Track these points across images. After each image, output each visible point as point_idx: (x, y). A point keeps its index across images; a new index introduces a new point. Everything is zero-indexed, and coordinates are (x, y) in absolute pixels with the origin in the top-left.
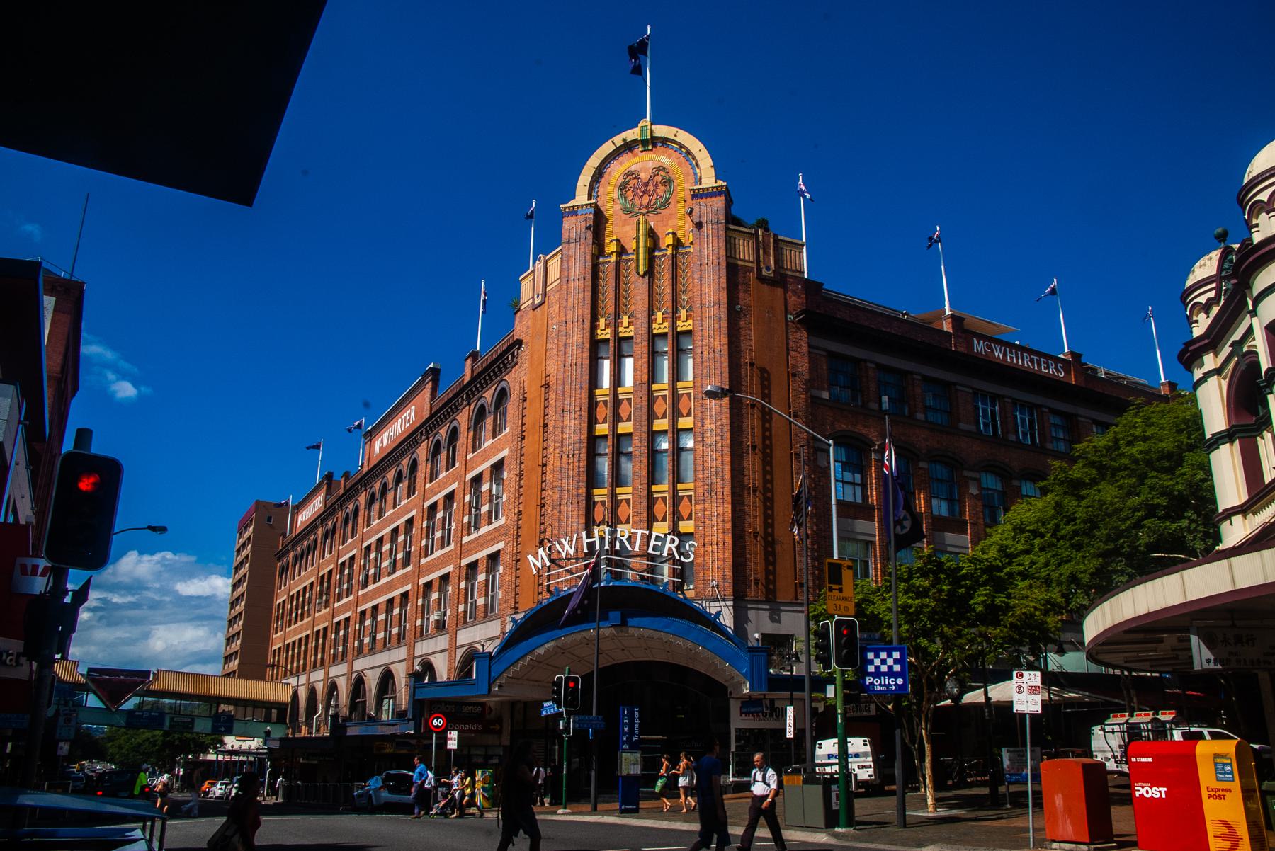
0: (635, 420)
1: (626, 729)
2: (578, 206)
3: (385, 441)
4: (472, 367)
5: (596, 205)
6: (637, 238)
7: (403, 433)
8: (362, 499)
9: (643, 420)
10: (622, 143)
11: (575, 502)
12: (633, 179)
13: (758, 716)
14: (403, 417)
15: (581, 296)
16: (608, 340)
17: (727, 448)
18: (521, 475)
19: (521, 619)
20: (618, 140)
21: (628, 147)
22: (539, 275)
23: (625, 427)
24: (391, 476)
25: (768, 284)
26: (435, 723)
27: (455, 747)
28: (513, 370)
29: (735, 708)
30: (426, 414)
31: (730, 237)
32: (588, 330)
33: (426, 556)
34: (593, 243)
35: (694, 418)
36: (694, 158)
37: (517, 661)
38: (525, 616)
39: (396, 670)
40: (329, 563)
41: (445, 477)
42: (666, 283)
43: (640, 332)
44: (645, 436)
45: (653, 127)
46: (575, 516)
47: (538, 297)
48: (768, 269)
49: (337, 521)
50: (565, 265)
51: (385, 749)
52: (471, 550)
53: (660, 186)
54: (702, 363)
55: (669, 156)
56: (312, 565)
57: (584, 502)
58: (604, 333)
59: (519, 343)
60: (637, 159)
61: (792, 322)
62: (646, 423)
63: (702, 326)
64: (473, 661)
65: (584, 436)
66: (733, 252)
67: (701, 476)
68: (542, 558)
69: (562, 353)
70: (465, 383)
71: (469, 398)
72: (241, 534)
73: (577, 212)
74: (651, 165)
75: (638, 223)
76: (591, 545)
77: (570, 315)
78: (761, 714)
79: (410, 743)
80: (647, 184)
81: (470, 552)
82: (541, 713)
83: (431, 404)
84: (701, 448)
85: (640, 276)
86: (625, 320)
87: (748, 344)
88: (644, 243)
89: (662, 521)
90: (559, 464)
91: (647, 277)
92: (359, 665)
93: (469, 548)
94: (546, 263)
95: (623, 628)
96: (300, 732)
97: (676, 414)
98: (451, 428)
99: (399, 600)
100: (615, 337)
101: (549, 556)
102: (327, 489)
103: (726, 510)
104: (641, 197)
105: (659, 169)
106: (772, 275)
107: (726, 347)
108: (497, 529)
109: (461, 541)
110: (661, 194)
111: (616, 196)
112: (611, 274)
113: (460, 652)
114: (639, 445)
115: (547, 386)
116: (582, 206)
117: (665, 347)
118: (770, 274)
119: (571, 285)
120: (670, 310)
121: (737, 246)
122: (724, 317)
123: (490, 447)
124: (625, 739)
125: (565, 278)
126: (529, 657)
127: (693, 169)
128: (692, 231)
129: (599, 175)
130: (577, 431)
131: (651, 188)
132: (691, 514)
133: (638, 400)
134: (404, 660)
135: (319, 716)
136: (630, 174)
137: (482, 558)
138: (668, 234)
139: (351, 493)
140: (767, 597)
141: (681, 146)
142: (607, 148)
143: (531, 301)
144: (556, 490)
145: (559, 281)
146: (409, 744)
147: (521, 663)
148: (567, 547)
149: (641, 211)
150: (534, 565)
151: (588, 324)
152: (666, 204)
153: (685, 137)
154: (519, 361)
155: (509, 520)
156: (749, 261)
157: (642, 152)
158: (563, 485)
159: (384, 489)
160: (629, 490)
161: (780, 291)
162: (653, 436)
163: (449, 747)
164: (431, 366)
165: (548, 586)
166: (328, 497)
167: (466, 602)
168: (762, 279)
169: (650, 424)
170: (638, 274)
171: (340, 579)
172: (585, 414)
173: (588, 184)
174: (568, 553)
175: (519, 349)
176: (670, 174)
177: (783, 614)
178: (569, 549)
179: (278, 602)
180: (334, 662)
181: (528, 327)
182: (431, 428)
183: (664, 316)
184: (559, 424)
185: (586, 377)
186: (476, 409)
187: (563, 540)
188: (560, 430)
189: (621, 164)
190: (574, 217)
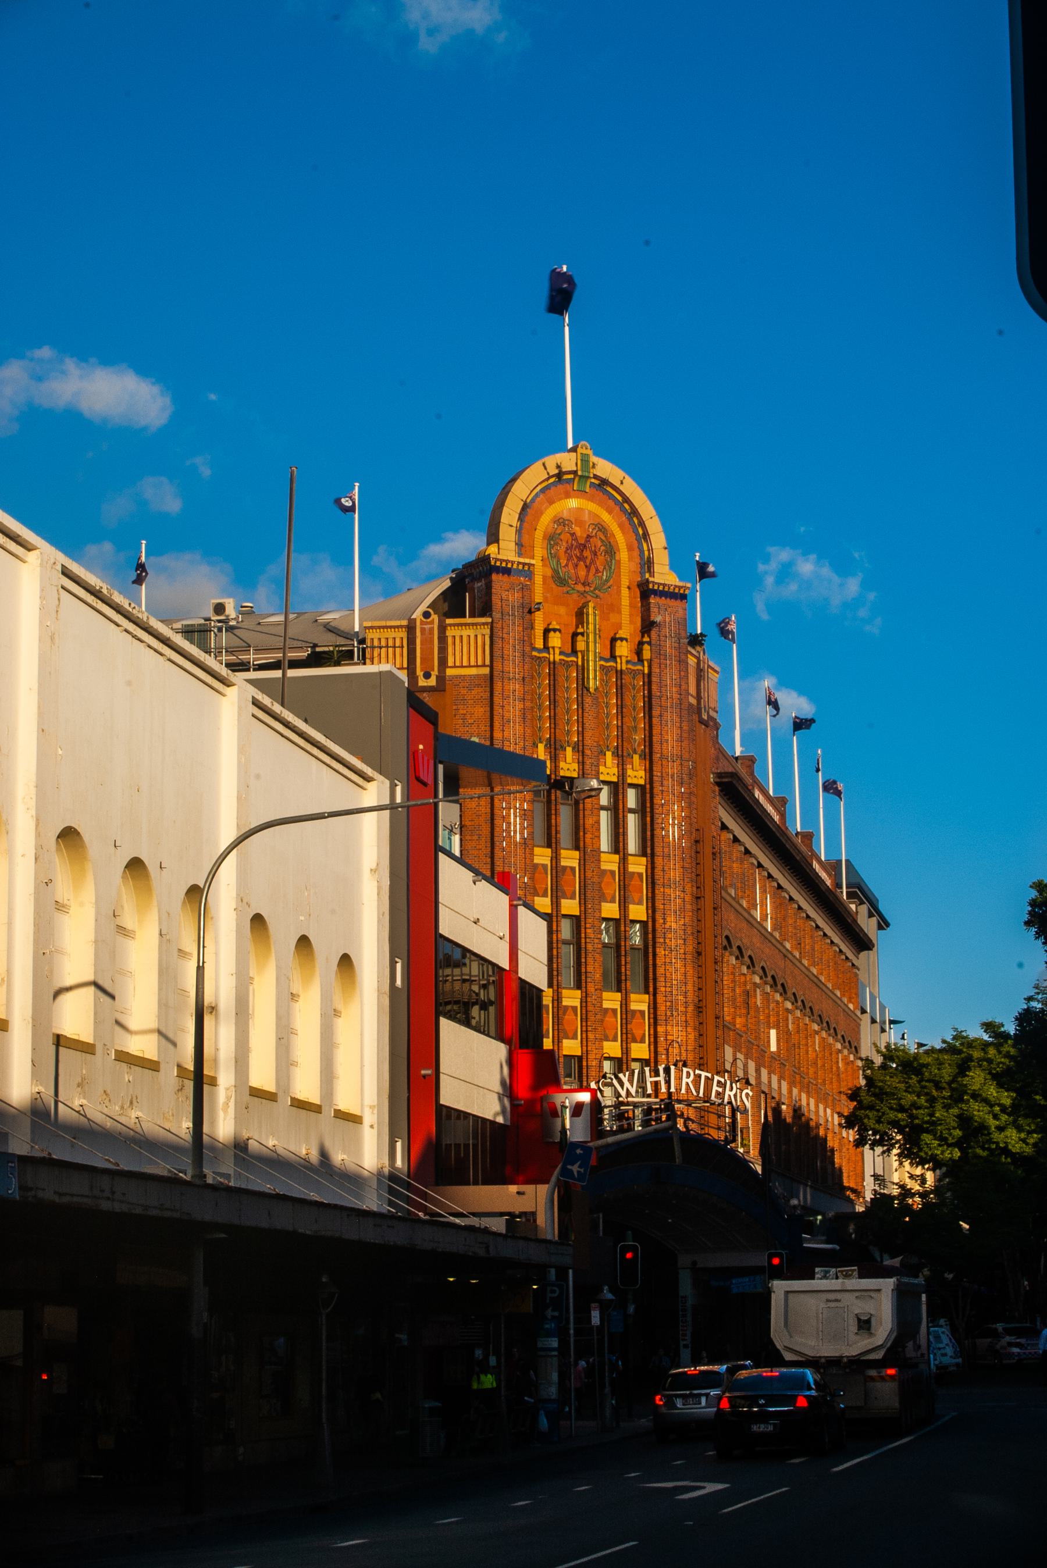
22: (427, 642)
36: (642, 524)
47: (427, 676)
84: (663, 952)
89: (612, 1041)
110: (601, 568)
131: (587, 553)
136: (560, 521)
141: (626, 500)
148: (627, 1084)
153: (632, 489)
187: (621, 1075)
190: (505, 578)
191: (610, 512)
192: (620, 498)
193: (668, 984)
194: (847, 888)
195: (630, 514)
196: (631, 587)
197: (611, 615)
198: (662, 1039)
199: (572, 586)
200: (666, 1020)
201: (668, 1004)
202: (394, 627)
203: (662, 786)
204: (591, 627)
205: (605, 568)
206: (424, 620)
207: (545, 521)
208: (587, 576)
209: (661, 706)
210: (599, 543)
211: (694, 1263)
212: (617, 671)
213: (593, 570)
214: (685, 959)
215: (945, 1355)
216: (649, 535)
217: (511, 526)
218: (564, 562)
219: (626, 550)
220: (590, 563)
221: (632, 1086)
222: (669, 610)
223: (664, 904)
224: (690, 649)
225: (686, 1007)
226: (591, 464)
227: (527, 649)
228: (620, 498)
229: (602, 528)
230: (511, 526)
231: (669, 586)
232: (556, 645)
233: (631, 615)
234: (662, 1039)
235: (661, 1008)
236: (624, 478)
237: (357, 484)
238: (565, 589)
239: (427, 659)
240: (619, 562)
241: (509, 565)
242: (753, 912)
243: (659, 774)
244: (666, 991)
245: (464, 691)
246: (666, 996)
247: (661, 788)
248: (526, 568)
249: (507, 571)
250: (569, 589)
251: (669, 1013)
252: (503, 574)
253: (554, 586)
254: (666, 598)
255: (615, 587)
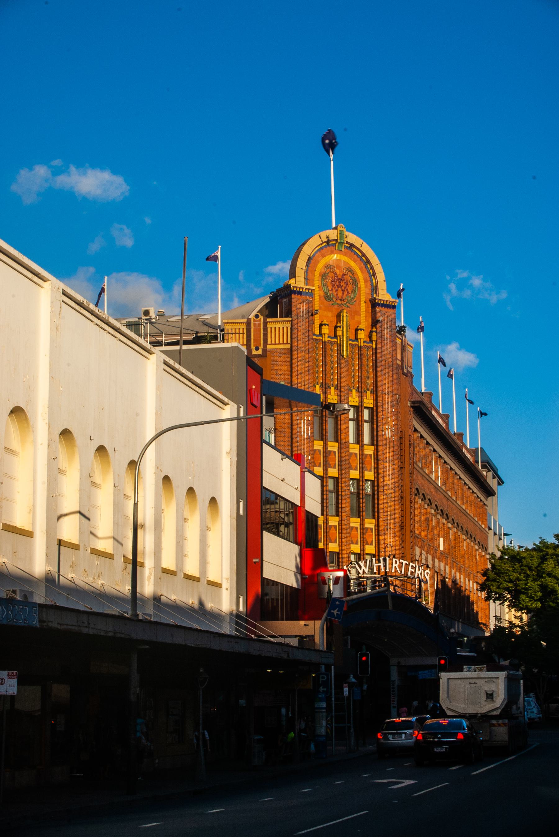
22: (257, 331)
36: (372, 268)
47: (257, 349)
63: (382, 408)
89: (355, 544)
110: (350, 291)
131: (342, 284)
141: (364, 255)
148: (363, 567)
176: (356, 277)
187: (360, 562)
190: (299, 297)
191: (355, 261)
192: (360, 254)
193: (385, 514)
194: (481, 463)
195: (365, 263)
196: (366, 301)
198: (382, 543)
199: (335, 301)
200: (384, 533)
201: (386, 524)
202: (240, 323)
203: (382, 408)
204: (345, 323)
205: (352, 292)
206: (256, 319)
207: (320, 266)
208: (343, 296)
209: (382, 365)
210: (349, 278)
211: (399, 663)
212: (358, 347)
213: (346, 292)
215: (533, 712)
216: (376, 274)
217: (302, 269)
218: (330, 288)
219: (363, 282)
220: (344, 289)
221: (366, 568)
222: (387, 314)
223: (383, 471)
224: (397, 335)
225: (395, 526)
226: (345, 236)
227: (311, 335)
228: (360, 254)
229: (350, 270)
230: (302, 269)
231: (386, 301)
232: (326, 333)
233: (366, 317)
234: (382, 543)
235: (382, 527)
236: (363, 243)
237: (220, 246)
238: (331, 303)
239: (257, 340)
240: (359, 289)
241: (301, 290)
242: (431, 475)
243: (381, 402)
244: (384, 518)
245: (277, 357)
246: (384, 520)
247: (382, 409)
248: (310, 291)
249: (300, 293)
250: (333, 302)
251: (386, 529)
252: (298, 295)
253: (325, 301)
254: (385, 308)
255: (358, 302)
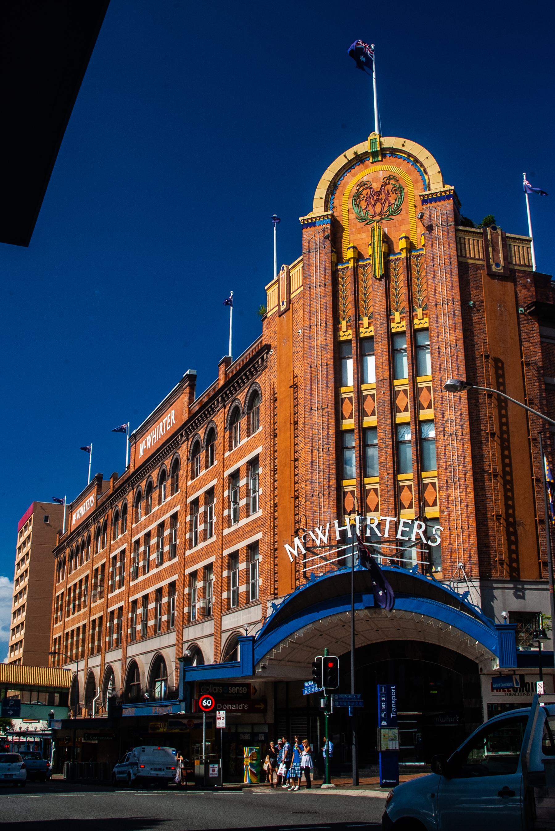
0: (379, 414)
1: (384, 706)
2: (316, 218)
3: (149, 444)
4: (226, 372)
5: (332, 215)
6: (372, 244)
7: (165, 435)
8: (130, 497)
9: (387, 414)
10: (354, 156)
11: (327, 493)
12: (366, 189)
13: (509, 691)
14: (164, 421)
15: (323, 301)
16: (349, 341)
17: (467, 437)
18: (275, 470)
19: (281, 604)
20: (350, 154)
21: (360, 159)
23: (370, 421)
24: (155, 475)
25: (498, 280)
26: (204, 703)
27: (224, 726)
28: (264, 373)
29: (486, 684)
30: (185, 417)
31: (460, 238)
32: (331, 333)
33: (190, 548)
34: (332, 251)
35: (435, 410)
36: (422, 165)
37: (279, 643)
38: (284, 602)
39: (167, 654)
40: (102, 557)
41: (204, 475)
42: (402, 284)
43: (380, 332)
44: (389, 428)
45: (382, 139)
46: (327, 506)
47: (283, 304)
48: (497, 265)
49: (108, 519)
50: (307, 274)
51: (158, 728)
52: (231, 541)
53: (391, 193)
54: (440, 357)
55: (399, 165)
56: (87, 560)
57: (335, 492)
58: (346, 334)
59: (268, 347)
60: (367, 171)
61: (523, 314)
62: (389, 416)
63: (437, 323)
64: (237, 645)
65: (332, 431)
66: (463, 251)
67: (443, 464)
68: (298, 547)
69: (308, 355)
70: (220, 386)
71: (223, 400)
72: (21, 533)
73: (315, 223)
74: (381, 175)
75: (373, 230)
76: (343, 533)
77: (314, 320)
78: (511, 689)
79: (181, 723)
80: (379, 193)
81: (231, 543)
82: (302, 692)
83: (189, 408)
84: (443, 438)
85: (377, 279)
86: (365, 321)
87: (482, 337)
88: (379, 248)
89: (408, 508)
90: (310, 458)
91: (383, 280)
92: (133, 650)
93: (230, 539)
94: (289, 272)
95: (377, 610)
96: (80, 713)
97: (417, 407)
98: (208, 429)
99: (167, 590)
100: (356, 337)
101: (305, 544)
102: (97, 490)
103: (469, 495)
104: (374, 205)
105: (389, 178)
106: (502, 271)
107: (462, 341)
108: (255, 521)
109: (222, 534)
110: (393, 202)
111: (350, 206)
112: (350, 280)
113: (225, 636)
114: (384, 437)
115: (295, 386)
116: (320, 217)
117: (404, 344)
118: (500, 270)
119: (314, 291)
120: (407, 310)
121: (467, 246)
122: (458, 313)
123: (245, 445)
124: (383, 715)
125: (307, 285)
126: (289, 640)
127: (422, 175)
128: (423, 234)
129: (333, 187)
130: (326, 427)
131: (383, 196)
132: (436, 500)
133: (381, 395)
134: (174, 645)
135: (99, 698)
137: (242, 548)
138: (401, 238)
139: (119, 492)
140: (511, 575)
141: (409, 155)
142: (340, 162)
143: (277, 308)
144: (308, 483)
145: (302, 287)
146: (181, 724)
147: (282, 645)
148: (321, 535)
149: (374, 219)
150: (291, 553)
151: (330, 327)
152: (397, 211)
154: (269, 364)
155: (266, 512)
156: (479, 259)
157: (372, 163)
158: (314, 478)
159: (150, 487)
160: (377, 479)
161: (510, 285)
162: (396, 427)
163: (218, 726)
164: (188, 372)
165: (305, 572)
166: (99, 496)
167: (229, 590)
168: (492, 275)
169: (393, 417)
170: (375, 277)
171: (113, 572)
172: (332, 411)
173: (324, 196)
174: (321, 541)
175: (267, 353)
176: (401, 182)
177: (527, 592)
178: (323, 537)
179: (57, 595)
180: (109, 648)
181: (275, 332)
182: (190, 430)
183: (401, 316)
184: (308, 420)
185: (331, 376)
186: (231, 411)
187: (317, 529)
188: (309, 426)
189: (354, 175)
190: (313, 228)
193: (448, 460)
197: (402, 227)
213: (387, 204)
214: (463, 439)
220: (385, 201)
221: (324, 535)
228: (406, 156)
230: (322, 198)
234: (444, 500)
238: (365, 223)
247: (436, 325)
251: (449, 481)
254: (436, 202)
